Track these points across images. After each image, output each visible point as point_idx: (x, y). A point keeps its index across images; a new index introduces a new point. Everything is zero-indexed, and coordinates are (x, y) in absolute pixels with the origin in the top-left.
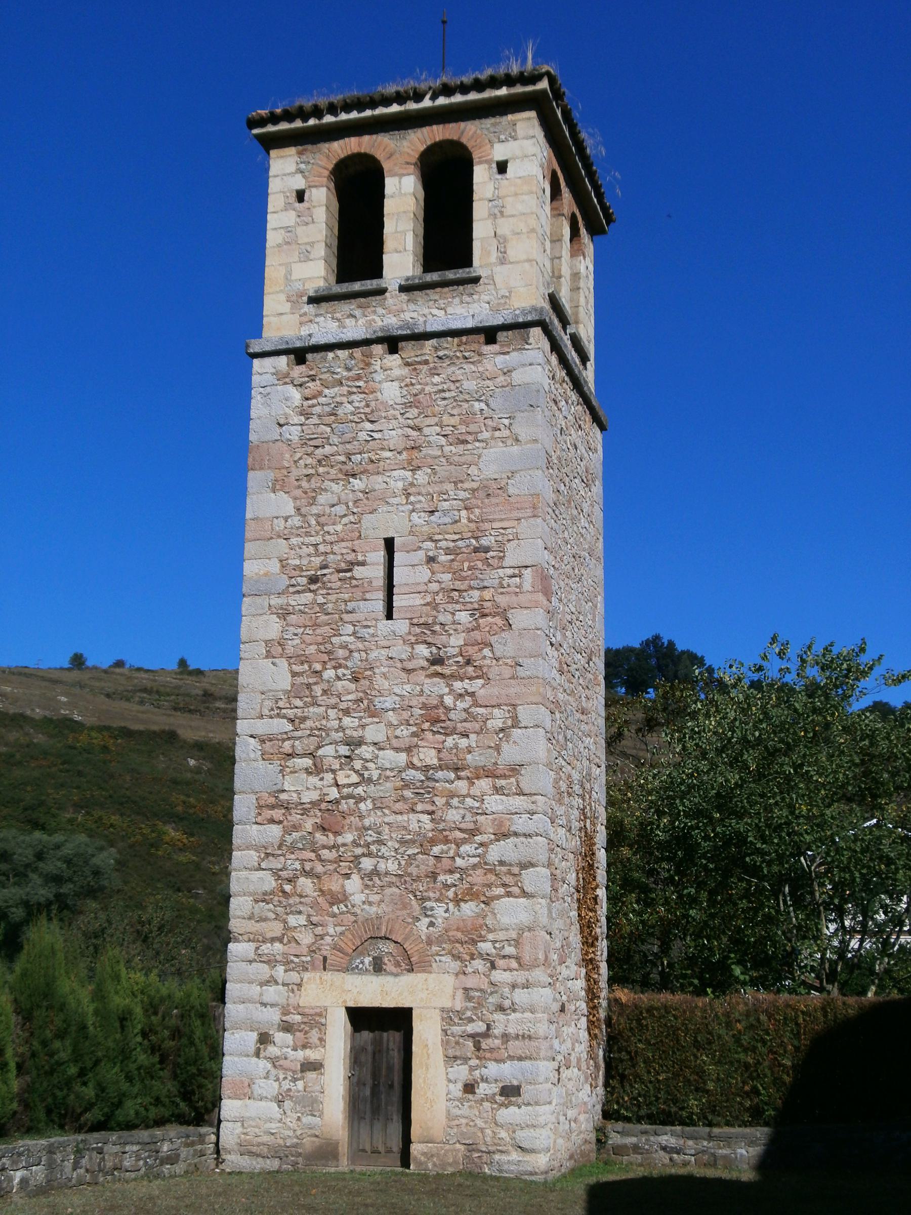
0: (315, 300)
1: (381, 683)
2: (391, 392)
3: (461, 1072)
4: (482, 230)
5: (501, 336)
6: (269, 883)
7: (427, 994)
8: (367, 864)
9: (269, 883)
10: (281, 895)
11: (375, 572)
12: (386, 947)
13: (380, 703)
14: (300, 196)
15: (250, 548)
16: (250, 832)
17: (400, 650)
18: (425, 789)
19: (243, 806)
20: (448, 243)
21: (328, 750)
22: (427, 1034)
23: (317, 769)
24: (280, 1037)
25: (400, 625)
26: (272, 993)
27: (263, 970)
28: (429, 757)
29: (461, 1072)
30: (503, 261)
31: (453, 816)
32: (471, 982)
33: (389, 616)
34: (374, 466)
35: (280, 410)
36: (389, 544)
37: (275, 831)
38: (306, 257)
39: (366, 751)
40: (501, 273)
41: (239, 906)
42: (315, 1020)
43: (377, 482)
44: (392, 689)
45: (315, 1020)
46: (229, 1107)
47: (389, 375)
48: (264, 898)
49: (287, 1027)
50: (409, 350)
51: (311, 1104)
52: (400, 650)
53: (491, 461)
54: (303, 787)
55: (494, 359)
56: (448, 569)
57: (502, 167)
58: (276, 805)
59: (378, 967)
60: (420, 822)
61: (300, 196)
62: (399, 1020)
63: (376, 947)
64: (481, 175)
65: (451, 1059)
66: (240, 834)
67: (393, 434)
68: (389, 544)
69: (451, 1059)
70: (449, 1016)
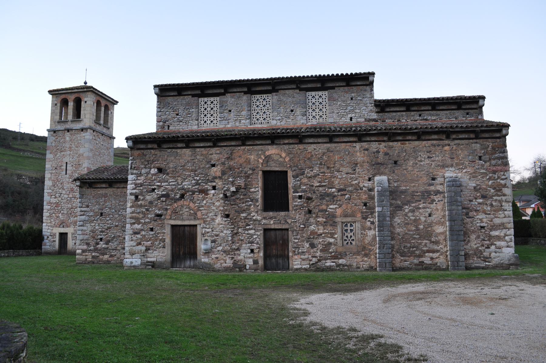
0: (58, 122)
1: (65, 185)
2: (68, 139)
3: (74, 241)
4: (82, 112)
5: (84, 130)
6: (49, 215)
7: (69, 230)
8: (62, 212)
9: (49, 215)
10: (50, 216)
11: (64, 167)
12: (64, 224)
13: (65, 188)
14: (56, 104)
15: (47, 163)
16: (46, 207)
17: (68, 180)
18: (70, 201)
19: (45, 203)
20: (78, 114)
21: (57, 195)
22: (69, 236)
23: (56, 198)
24: (50, 237)
25: (67, 176)
26: (49, 231)
27: (47, 227)
28: (71, 196)
29: (74, 241)
30: (85, 118)
31: (74, 205)
32: (75, 229)
33: (66, 174)
34: (65, 151)
35: (51, 141)
36: (67, 163)
37: (49, 207)
38: (56, 115)
39: (62, 195)
40: (85, 120)
41: (44, 218)
42: (55, 235)
43: (65, 153)
44: (66, 186)
45: (55, 235)
46: (43, 247)
47: (68, 136)
48: (48, 217)
49: (51, 236)
50: (71, 132)
51: (54, 246)
52: (68, 180)
53: (81, 150)
54: (53, 200)
55: (83, 134)
56: (75, 167)
57: (86, 102)
58: (49, 203)
59: (63, 227)
60: (70, 206)
61: (56, 104)
62: (66, 234)
63: (62, 224)
64: (83, 103)
65: (73, 240)
66: (44, 207)
67: (67, 145)
68: (67, 163)
69: (73, 240)
70: (73, 234)
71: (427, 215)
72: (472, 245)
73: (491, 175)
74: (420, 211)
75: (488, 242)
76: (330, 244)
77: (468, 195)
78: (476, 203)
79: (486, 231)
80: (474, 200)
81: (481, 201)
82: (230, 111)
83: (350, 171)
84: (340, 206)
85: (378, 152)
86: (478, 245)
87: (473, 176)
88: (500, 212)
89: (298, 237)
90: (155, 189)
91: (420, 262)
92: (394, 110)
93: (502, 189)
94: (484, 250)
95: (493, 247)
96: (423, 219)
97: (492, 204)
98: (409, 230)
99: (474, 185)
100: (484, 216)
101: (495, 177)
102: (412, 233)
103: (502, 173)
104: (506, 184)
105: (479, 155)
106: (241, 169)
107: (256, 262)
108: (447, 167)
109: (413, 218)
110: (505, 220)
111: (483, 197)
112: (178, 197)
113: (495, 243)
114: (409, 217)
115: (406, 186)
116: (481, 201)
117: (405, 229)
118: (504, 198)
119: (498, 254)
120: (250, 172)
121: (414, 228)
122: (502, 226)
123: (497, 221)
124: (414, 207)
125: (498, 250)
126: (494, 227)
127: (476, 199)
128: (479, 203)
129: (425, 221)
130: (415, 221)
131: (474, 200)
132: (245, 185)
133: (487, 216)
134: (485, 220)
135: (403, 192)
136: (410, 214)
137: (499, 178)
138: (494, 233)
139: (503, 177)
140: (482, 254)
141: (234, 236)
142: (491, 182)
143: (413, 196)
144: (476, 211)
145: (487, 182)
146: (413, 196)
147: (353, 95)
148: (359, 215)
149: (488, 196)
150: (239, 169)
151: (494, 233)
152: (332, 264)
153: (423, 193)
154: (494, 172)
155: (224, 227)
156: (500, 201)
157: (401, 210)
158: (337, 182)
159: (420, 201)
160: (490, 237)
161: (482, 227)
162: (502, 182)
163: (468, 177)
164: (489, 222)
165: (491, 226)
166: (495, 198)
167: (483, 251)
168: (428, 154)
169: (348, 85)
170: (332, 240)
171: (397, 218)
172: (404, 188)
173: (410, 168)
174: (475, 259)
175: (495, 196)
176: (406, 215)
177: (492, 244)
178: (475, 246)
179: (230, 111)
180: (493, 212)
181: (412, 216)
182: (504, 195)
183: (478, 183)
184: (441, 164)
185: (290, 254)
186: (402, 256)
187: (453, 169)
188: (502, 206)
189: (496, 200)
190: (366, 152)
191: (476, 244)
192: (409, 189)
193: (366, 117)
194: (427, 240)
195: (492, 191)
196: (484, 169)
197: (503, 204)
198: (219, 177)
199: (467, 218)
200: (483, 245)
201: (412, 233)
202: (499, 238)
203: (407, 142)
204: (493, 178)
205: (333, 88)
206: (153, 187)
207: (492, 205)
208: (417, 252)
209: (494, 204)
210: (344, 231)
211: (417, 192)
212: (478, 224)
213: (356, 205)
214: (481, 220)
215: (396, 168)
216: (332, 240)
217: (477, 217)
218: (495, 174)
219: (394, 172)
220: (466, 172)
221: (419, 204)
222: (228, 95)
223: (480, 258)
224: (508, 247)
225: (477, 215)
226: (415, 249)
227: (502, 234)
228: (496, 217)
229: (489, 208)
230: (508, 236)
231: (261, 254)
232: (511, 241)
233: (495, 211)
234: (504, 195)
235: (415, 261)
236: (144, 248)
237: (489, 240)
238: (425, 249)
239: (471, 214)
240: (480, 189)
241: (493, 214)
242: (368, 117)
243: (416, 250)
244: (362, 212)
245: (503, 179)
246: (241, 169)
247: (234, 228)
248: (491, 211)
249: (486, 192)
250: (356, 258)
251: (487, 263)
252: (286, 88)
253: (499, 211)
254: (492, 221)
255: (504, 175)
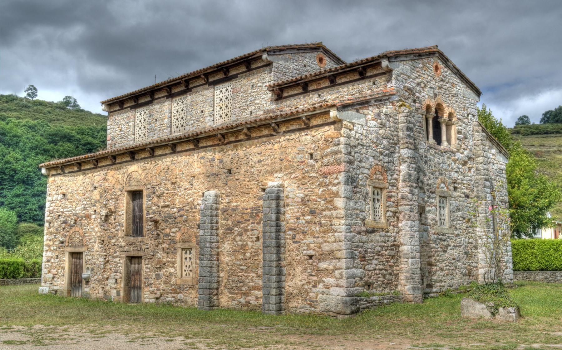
71: (255, 239)
72: (297, 281)
73: (321, 180)
74: (248, 233)
75: (315, 278)
76: (171, 274)
77: (296, 210)
78: (304, 221)
79: (314, 262)
80: (302, 218)
81: (308, 218)
82: (156, 120)
83: (188, 186)
84: (180, 228)
85: (213, 160)
86: (304, 282)
87: (301, 182)
88: (330, 234)
89: (149, 266)
90: (59, 216)
91: (246, 302)
92: (290, 94)
93: (333, 201)
94: (310, 289)
95: (321, 286)
96: (250, 244)
97: (321, 223)
98: (237, 260)
99: (302, 195)
100: (312, 240)
101: (325, 183)
102: (238, 262)
103: (335, 176)
104: (338, 192)
105: (310, 151)
106: (113, 190)
107: (118, 294)
108: (276, 172)
109: (240, 243)
110: (335, 246)
111: (312, 213)
112: (72, 223)
113: (324, 279)
114: (237, 242)
115: (236, 202)
116: (308, 218)
117: (233, 257)
118: (334, 213)
119: (324, 297)
120: (119, 193)
121: (241, 257)
122: (331, 255)
123: (326, 247)
124: (243, 228)
125: (325, 290)
126: (323, 256)
127: (304, 215)
128: (307, 222)
129: (252, 248)
130: (243, 247)
131: (302, 218)
132: (116, 208)
133: (315, 240)
134: (312, 246)
135: (234, 210)
136: (238, 238)
137: (330, 183)
138: (323, 265)
139: (336, 181)
140: (308, 295)
141: (107, 264)
142: (321, 190)
143: (243, 214)
144: (304, 233)
145: (316, 191)
146: (243, 214)
147: (254, 81)
148: (194, 240)
149: (317, 211)
150: (111, 190)
151: (323, 265)
152: (173, 299)
153: (252, 209)
154: (325, 175)
155: (99, 255)
156: (330, 217)
157: (230, 233)
158: (178, 200)
159: (249, 220)
160: (319, 271)
161: (311, 257)
162: (334, 189)
163: (296, 185)
164: (317, 249)
165: (319, 255)
166: (324, 213)
167: (309, 290)
168: (259, 157)
169: (249, 69)
170: (172, 270)
171: (227, 243)
172: (235, 204)
173: (242, 178)
174: (300, 301)
175: (324, 210)
176: (234, 239)
177: (320, 281)
178: (300, 283)
179: (156, 120)
180: (322, 234)
181: (240, 241)
182: (336, 208)
183: (306, 193)
184: (269, 169)
185: (143, 286)
186: (231, 293)
187: (280, 175)
188: (331, 225)
189: (325, 216)
190: (202, 161)
191: (301, 281)
192: (239, 205)
193: (264, 109)
194: (254, 272)
195: (323, 202)
196: (314, 172)
197: (334, 221)
198: (98, 200)
199: (294, 242)
200: (309, 283)
201: (238, 262)
202: (328, 272)
203: (239, 143)
204: (324, 184)
205: (235, 77)
206: (59, 214)
207: (320, 224)
208: (244, 289)
209: (323, 222)
210: (184, 260)
211: (247, 209)
212: (305, 252)
213: (191, 228)
214: (308, 245)
215: (229, 178)
216: (172, 270)
217: (304, 241)
218: (326, 178)
219: (227, 184)
220: (294, 178)
221: (248, 225)
222: (155, 102)
223: (306, 300)
224: (337, 286)
225: (305, 238)
226: (242, 284)
227: (331, 267)
228: (325, 242)
229: (318, 229)
230: (337, 269)
231: (122, 285)
232: (341, 278)
233: (324, 232)
234: (336, 208)
235: (242, 300)
236: (51, 276)
237: (317, 275)
238: (251, 284)
239: (299, 237)
240: (308, 201)
241: (322, 237)
242: (267, 108)
243: (243, 286)
244: (196, 237)
245: (334, 185)
246: (113, 190)
247: (106, 256)
248: (320, 232)
249: (315, 204)
250: (191, 293)
251: (313, 309)
252: (198, 84)
253: (328, 233)
254: (320, 247)
255: (337, 178)
